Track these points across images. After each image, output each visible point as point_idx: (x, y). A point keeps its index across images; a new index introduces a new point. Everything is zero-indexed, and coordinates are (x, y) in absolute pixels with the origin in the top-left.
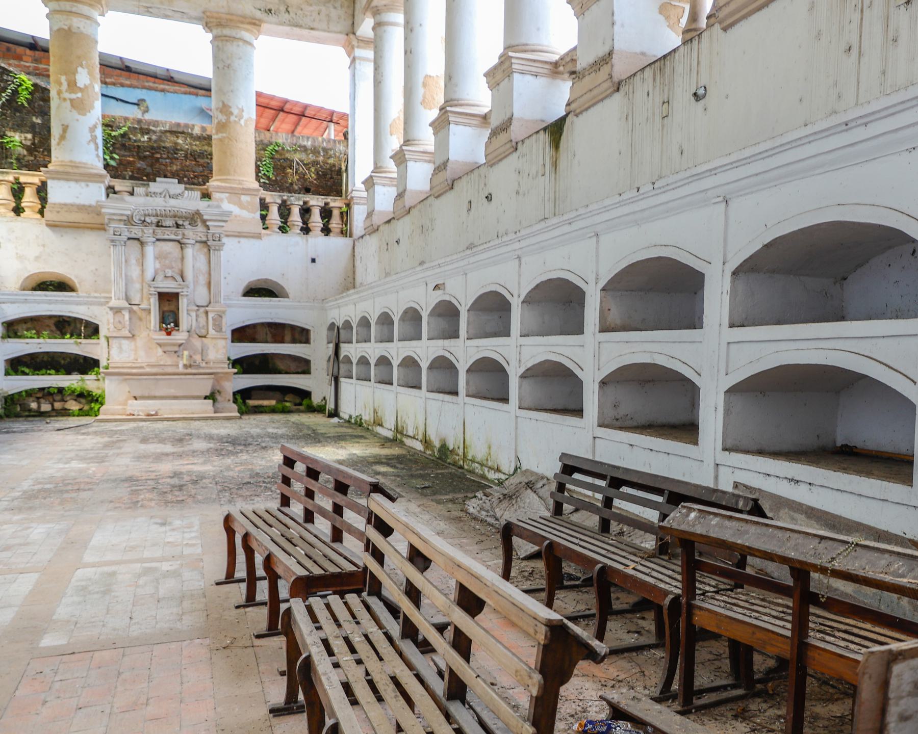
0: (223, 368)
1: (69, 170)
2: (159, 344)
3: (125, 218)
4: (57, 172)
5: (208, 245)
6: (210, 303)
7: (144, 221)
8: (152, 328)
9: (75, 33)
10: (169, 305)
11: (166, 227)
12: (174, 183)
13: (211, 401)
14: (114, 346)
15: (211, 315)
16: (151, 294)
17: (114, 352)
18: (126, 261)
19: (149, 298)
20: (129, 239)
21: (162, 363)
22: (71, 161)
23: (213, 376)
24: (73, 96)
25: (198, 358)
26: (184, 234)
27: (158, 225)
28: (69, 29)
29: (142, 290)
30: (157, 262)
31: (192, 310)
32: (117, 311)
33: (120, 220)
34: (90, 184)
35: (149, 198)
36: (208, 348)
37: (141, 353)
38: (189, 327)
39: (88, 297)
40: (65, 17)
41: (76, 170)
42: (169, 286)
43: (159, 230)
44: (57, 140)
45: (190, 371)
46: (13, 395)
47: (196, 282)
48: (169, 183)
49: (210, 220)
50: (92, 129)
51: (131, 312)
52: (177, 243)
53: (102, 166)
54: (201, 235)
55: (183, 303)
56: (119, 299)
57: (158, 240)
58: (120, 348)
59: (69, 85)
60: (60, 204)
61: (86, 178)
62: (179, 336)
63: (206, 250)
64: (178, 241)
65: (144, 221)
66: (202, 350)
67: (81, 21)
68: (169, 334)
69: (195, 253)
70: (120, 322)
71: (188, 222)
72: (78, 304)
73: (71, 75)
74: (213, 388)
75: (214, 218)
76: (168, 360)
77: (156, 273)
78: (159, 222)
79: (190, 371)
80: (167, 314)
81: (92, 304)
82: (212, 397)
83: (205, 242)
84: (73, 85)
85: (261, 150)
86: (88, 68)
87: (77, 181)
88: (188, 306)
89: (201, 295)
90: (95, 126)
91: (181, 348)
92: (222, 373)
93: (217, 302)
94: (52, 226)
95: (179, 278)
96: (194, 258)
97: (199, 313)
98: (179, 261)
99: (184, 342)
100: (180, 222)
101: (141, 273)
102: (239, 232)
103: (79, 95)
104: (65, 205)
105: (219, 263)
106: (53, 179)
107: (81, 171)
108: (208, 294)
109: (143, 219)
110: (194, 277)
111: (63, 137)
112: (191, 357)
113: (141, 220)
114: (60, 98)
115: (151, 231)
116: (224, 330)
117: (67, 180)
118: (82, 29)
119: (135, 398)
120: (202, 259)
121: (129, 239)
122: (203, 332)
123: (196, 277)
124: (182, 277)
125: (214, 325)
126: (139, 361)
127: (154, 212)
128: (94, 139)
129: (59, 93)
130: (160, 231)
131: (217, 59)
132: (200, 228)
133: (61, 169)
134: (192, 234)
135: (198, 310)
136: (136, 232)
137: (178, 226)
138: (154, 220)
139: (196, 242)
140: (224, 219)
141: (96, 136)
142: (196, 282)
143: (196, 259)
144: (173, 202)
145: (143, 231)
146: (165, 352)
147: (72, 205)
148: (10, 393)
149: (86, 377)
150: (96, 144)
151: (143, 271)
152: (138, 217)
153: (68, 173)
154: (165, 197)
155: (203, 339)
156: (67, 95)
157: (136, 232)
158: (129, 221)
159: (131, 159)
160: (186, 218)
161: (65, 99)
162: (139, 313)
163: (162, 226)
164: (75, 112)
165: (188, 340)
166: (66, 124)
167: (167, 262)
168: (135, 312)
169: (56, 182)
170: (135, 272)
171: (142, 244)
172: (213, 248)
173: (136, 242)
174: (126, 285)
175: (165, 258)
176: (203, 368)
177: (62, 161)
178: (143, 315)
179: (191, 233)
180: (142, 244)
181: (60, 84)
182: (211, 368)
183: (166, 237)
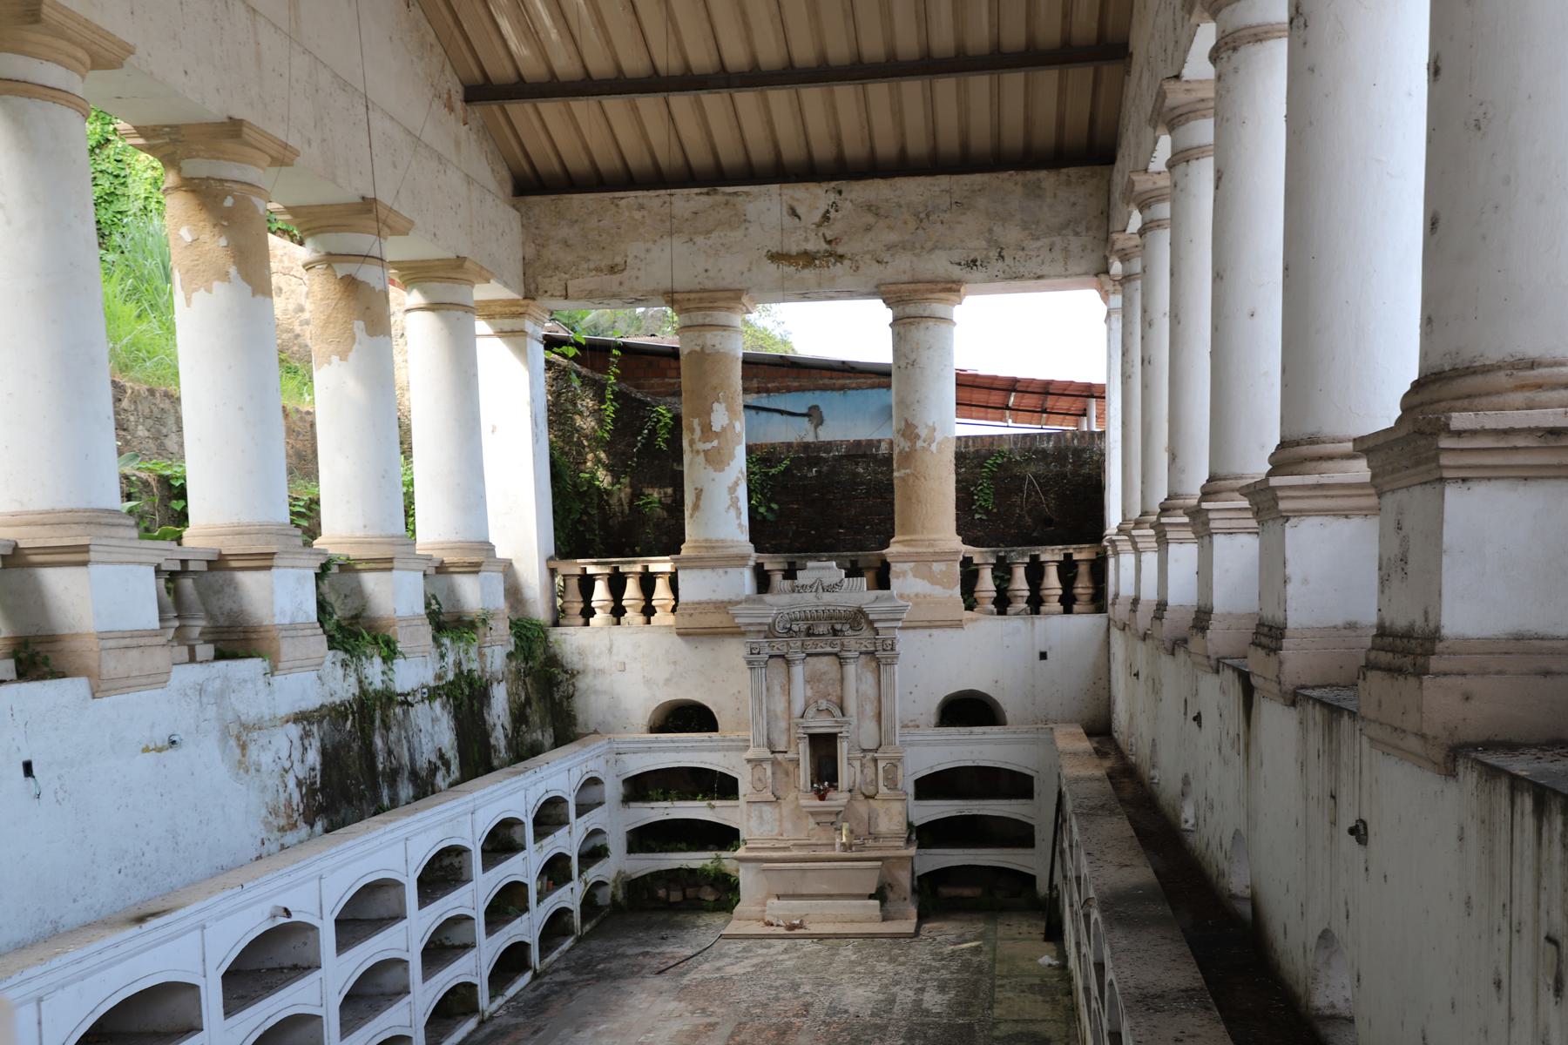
0: (898, 848)
1: (704, 554)
3: (766, 628)
4: (689, 559)
5: (880, 657)
6: (880, 745)
8: (802, 788)
9: (709, 355)
11: (819, 635)
13: (877, 902)
15: (881, 765)
16: (799, 738)
18: (768, 689)
21: (813, 841)
22: (706, 540)
23: (879, 863)
24: (708, 446)
25: (862, 830)
26: (843, 645)
27: (809, 632)
28: (702, 348)
29: (789, 729)
30: (809, 687)
31: (856, 759)
32: (756, 763)
33: (759, 632)
34: (729, 570)
35: (795, 595)
37: (788, 825)
39: (723, 741)
40: (696, 334)
41: (712, 554)
42: (822, 725)
43: (810, 641)
44: (690, 511)
46: (636, 879)
47: (861, 714)
48: (823, 568)
50: (732, 489)
51: (775, 763)
52: (834, 658)
53: (744, 537)
54: (866, 644)
55: (843, 749)
56: (759, 746)
57: (809, 655)
58: (761, 817)
59: (702, 431)
60: (694, 603)
61: (725, 563)
62: (838, 799)
63: (874, 664)
64: (836, 654)
65: (790, 629)
67: (716, 335)
68: (822, 798)
69: (859, 671)
71: (848, 626)
72: (712, 750)
73: (705, 413)
75: (883, 617)
76: (821, 836)
77: (807, 706)
78: (809, 628)
81: (728, 749)
82: (880, 894)
83: (872, 653)
84: (707, 429)
85: (976, 467)
86: (726, 401)
87: (713, 568)
89: (867, 733)
90: (736, 484)
91: (840, 816)
92: (894, 857)
94: (684, 634)
96: (859, 678)
97: (864, 761)
100: (838, 627)
102: (929, 621)
103: (715, 443)
104: (700, 603)
105: (892, 685)
106: (685, 568)
107: (719, 553)
109: (788, 626)
111: (696, 507)
112: (851, 832)
114: (692, 451)
115: (799, 643)
117: (702, 568)
118: (718, 346)
119: (778, 897)
120: (869, 678)
122: (870, 790)
123: (860, 706)
125: (886, 778)
126: (785, 837)
127: (803, 615)
128: (735, 503)
129: (692, 443)
130: (811, 643)
131: (896, 350)
132: (866, 633)
133: (693, 553)
134: (854, 642)
135: (864, 757)
136: (780, 646)
137: (835, 632)
138: (804, 627)
139: (861, 653)
140: (898, 616)
141: (737, 498)
143: (861, 679)
144: (827, 597)
145: (788, 644)
146: (818, 824)
147: (708, 603)
148: (634, 877)
149: (724, 854)
150: (738, 509)
151: (789, 702)
152: (781, 625)
153: (701, 559)
154: (816, 591)
155: (871, 801)
156: (701, 446)
157: (780, 646)
158: (770, 632)
160: (847, 619)
161: (698, 452)
163: (814, 635)
164: (710, 469)
166: (699, 487)
167: (821, 686)
168: (779, 763)
169: (688, 571)
170: (779, 705)
172: (883, 661)
173: (780, 660)
174: (768, 723)
175: (819, 681)
177: (696, 541)
178: (791, 767)
179: (853, 642)
180: (789, 663)
181: (692, 431)
182: (880, 848)
183: (819, 650)
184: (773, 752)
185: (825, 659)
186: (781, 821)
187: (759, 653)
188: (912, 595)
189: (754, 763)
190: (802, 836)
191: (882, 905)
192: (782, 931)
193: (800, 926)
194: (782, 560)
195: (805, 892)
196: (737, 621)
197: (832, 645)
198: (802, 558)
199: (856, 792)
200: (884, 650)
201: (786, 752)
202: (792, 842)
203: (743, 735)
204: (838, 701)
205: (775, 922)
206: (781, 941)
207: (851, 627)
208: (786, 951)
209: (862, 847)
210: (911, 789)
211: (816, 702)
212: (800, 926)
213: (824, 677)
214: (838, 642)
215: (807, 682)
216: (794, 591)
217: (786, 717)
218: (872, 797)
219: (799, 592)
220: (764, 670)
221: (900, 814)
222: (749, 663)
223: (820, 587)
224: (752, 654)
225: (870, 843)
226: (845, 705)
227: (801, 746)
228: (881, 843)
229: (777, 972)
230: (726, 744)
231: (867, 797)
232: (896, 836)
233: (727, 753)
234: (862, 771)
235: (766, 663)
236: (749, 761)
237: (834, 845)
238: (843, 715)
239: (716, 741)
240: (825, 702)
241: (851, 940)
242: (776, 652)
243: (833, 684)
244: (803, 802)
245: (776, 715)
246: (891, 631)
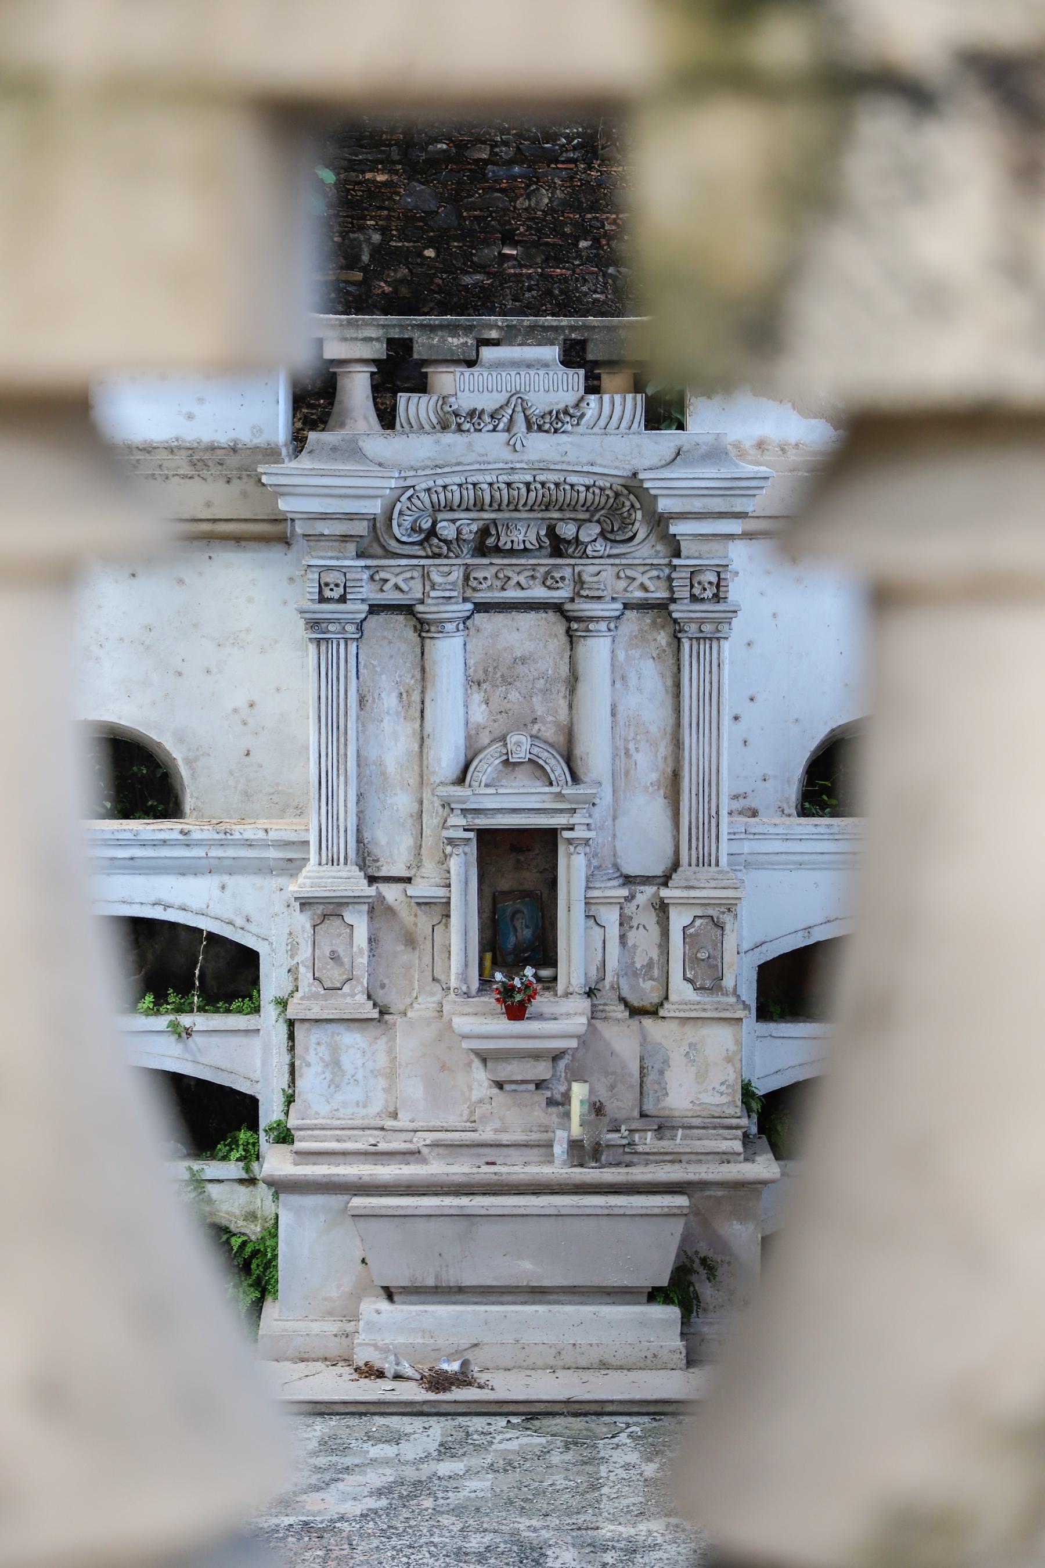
0: (725, 1157)
2: (477, 1053)
3: (361, 528)
6: (676, 866)
7: (432, 532)
8: (453, 983)
10: (518, 866)
11: (512, 552)
12: (546, 365)
13: (672, 1313)
14: (312, 1057)
15: (678, 920)
16: (451, 841)
17: (309, 1081)
18: (362, 701)
19: (446, 857)
20: (375, 609)
21: (487, 1134)
23: (681, 1201)
26: (579, 581)
30: (477, 697)
31: (608, 902)
33: (345, 538)
36: (666, 1062)
37: (413, 1089)
38: (593, 973)
43: (486, 569)
45: (590, 1174)
47: (621, 777)
49: (683, 516)
51: (377, 910)
52: (551, 616)
57: (482, 607)
58: (335, 1064)
63: (663, 638)
64: (558, 608)
65: (432, 532)
66: (642, 1076)
68: (516, 1012)
69: (621, 656)
70: (335, 957)
74: (682, 1251)
75: (697, 505)
78: (484, 532)
79: (590, 1174)
80: (509, 906)
83: (662, 607)
88: (588, 888)
91: (562, 1064)
93: (703, 862)
95: (557, 769)
96: (618, 676)
97: (630, 909)
98: (563, 690)
99: (573, 1044)
100: (567, 531)
101: (416, 747)
108: (667, 823)
109: (426, 525)
110: (615, 756)
112: (597, 1109)
113: (421, 531)
115: (457, 575)
116: (728, 982)
121: (375, 609)
122: (647, 992)
123: (621, 753)
124: (569, 759)
125: (691, 960)
130: (489, 573)
135: (630, 898)
137: (557, 546)
138: (470, 530)
139: (626, 606)
142: (621, 777)
145: (425, 576)
146: (500, 1085)
147: (171, 450)
152: (407, 524)
154: (508, 430)
155: (648, 1022)
159: (381, 178)
160: (592, 509)
162: (406, 915)
163: (497, 550)
165: (588, 1039)
167: (514, 695)
168: (390, 910)
171: (423, 627)
172: (692, 629)
174: (360, 797)
175: (507, 681)
176: (648, 1157)
178: (423, 923)
179: (608, 574)
180: (423, 627)
182: (676, 1159)
183: (512, 594)
184: (372, 880)
185: (527, 620)
186: (391, 1074)
187: (343, 599)
188: (748, 444)
189: (319, 909)
190: (453, 1121)
191: (686, 1321)
192: (412, 1392)
193: (463, 1379)
194: (372, 333)
195: (469, 1280)
196: (283, 505)
197: (549, 581)
198: (432, 328)
199: (607, 995)
200: (694, 598)
201: (408, 880)
202: (430, 1137)
203: (283, 829)
204: (561, 739)
205: (389, 1368)
206: (418, 1422)
207: (602, 534)
208: (446, 1450)
209: (628, 1154)
210: (749, 993)
211: (503, 739)
212: (463, 1379)
213: (522, 669)
214: (567, 572)
215: (473, 683)
216: (445, 427)
217: (413, 780)
218: (652, 1012)
219: (459, 429)
220: (353, 647)
221: (729, 1060)
222: (314, 624)
223: (520, 419)
224: (322, 599)
225: (648, 1141)
226: (579, 751)
227: (455, 864)
228: (679, 1142)
229: (457, 1511)
230: (231, 852)
231: (635, 1012)
232: (716, 1124)
233: (226, 879)
234: (623, 937)
235: (360, 626)
236: (305, 903)
237: (549, 1145)
238: (575, 779)
239: (199, 843)
240: (525, 741)
241: (621, 1420)
242: (391, 596)
243: (545, 691)
244: (463, 1024)
245: (383, 774)
246: (715, 546)
